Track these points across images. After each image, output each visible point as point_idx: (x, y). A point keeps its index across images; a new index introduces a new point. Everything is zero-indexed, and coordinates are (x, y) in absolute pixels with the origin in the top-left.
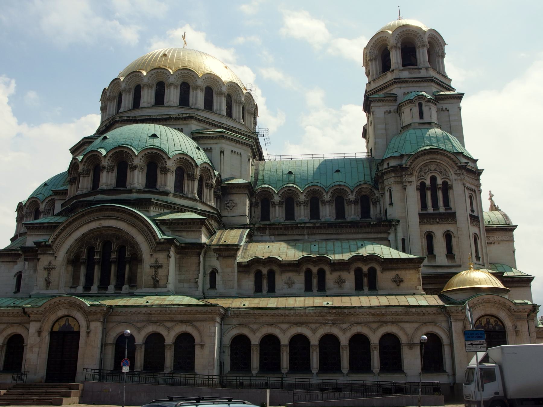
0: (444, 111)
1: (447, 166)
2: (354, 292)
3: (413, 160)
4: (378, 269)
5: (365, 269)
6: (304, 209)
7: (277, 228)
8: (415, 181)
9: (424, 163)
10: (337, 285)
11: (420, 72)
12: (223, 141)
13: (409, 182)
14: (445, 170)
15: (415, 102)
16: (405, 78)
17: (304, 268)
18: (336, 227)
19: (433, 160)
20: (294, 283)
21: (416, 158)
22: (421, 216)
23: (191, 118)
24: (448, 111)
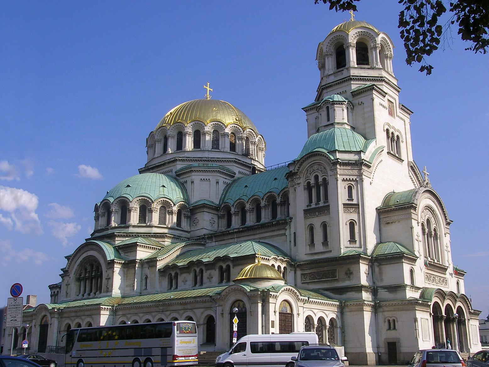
0: (360, 105)
1: (325, 164)
2: (217, 285)
3: (300, 165)
4: (231, 266)
5: (224, 266)
6: (250, 215)
7: (219, 236)
8: (302, 182)
9: (309, 165)
10: (208, 281)
11: (342, 74)
12: (193, 174)
13: (298, 184)
14: (325, 168)
15: (323, 107)
16: (329, 84)
17: (193, 270)
18: (252, 230)
19: (315, 162)
20: (186, 281)
21: (302, 163)
22: (305, 211)
23: (175, 161)
24: (364, 104)
